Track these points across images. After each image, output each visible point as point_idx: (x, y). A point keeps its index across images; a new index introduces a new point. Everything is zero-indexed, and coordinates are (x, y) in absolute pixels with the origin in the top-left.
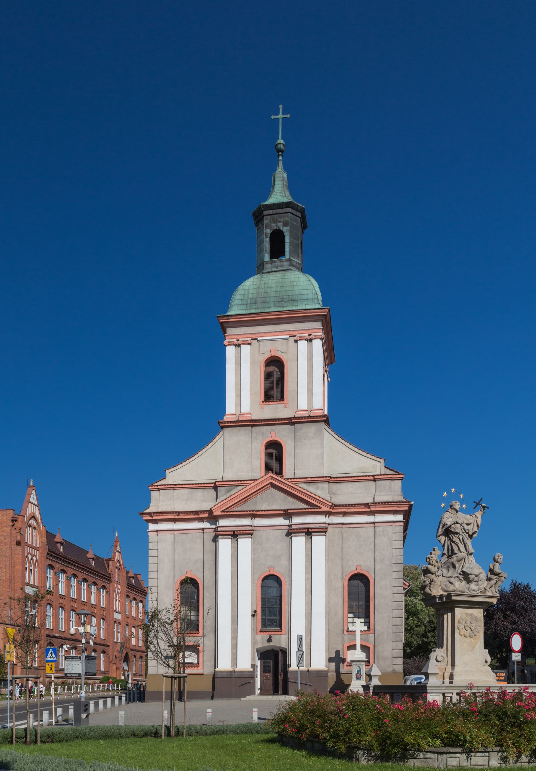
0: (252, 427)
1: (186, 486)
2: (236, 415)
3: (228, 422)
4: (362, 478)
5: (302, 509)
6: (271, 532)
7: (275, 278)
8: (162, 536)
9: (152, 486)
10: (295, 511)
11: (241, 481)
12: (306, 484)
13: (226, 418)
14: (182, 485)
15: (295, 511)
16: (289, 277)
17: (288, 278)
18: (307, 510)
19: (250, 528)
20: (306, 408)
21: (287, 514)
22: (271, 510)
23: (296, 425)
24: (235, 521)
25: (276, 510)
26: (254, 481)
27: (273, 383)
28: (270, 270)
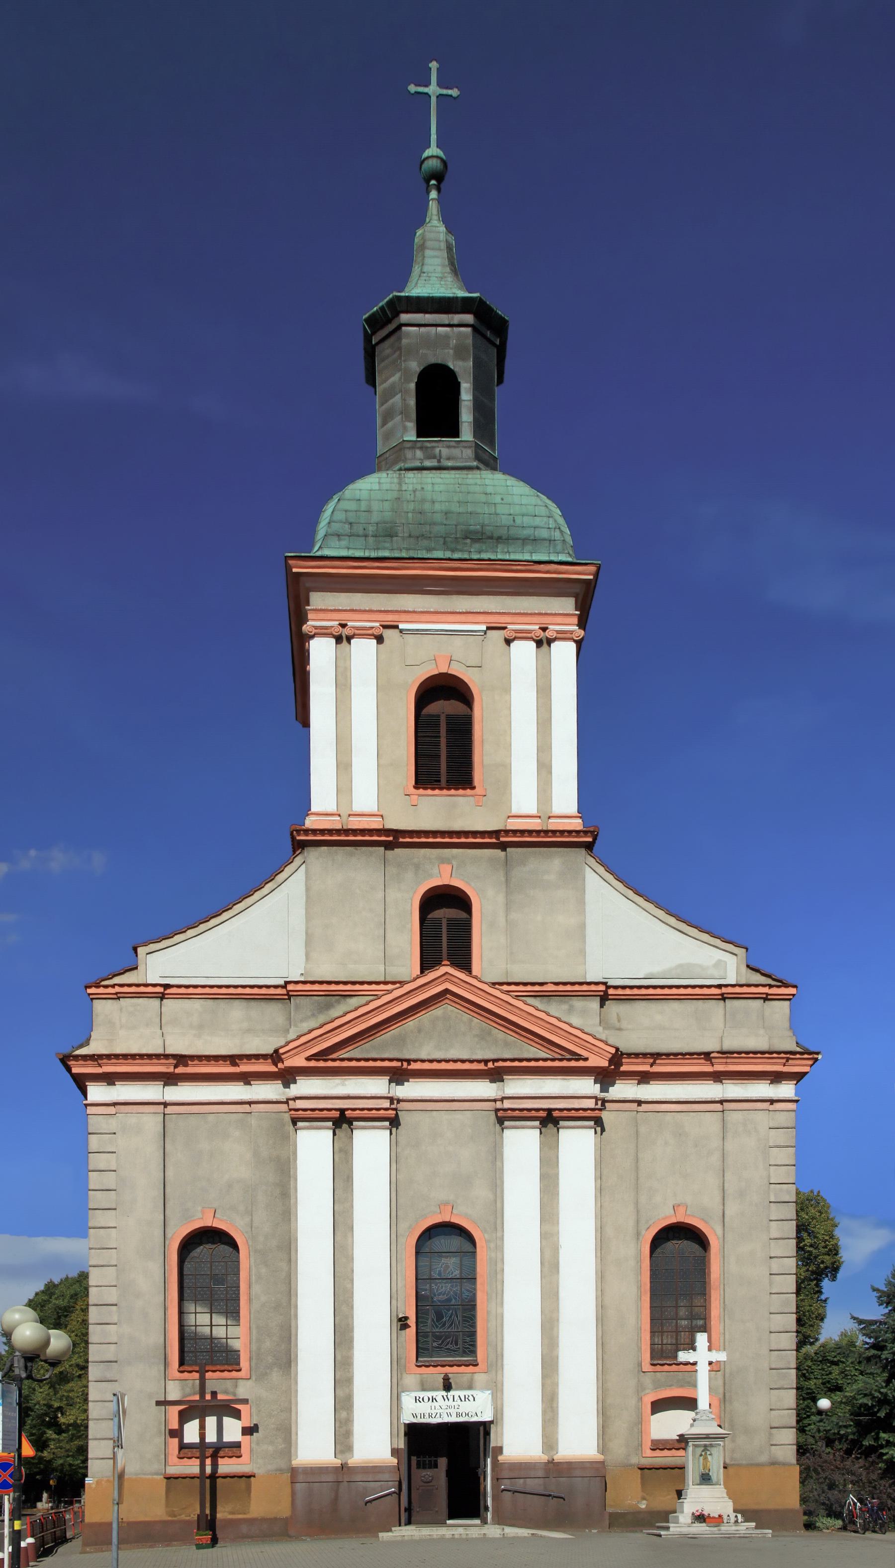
0: (386, 849)
1: (199, 990)
2: (339, 815)
3: (315, 832)
7: (439, 480)
8: (131, 1118)
9: (98, 987)
12: (538, 998)
13: (310, 822)
14: (187, 987)
16: (479, 481)
17: (476, 484)
18: (549, 1064)
19: (386, 1104)
20: (534, 812)
23: (508, 849)
24: (343, 1085)
27: (438, 744)
28: (418, 464)
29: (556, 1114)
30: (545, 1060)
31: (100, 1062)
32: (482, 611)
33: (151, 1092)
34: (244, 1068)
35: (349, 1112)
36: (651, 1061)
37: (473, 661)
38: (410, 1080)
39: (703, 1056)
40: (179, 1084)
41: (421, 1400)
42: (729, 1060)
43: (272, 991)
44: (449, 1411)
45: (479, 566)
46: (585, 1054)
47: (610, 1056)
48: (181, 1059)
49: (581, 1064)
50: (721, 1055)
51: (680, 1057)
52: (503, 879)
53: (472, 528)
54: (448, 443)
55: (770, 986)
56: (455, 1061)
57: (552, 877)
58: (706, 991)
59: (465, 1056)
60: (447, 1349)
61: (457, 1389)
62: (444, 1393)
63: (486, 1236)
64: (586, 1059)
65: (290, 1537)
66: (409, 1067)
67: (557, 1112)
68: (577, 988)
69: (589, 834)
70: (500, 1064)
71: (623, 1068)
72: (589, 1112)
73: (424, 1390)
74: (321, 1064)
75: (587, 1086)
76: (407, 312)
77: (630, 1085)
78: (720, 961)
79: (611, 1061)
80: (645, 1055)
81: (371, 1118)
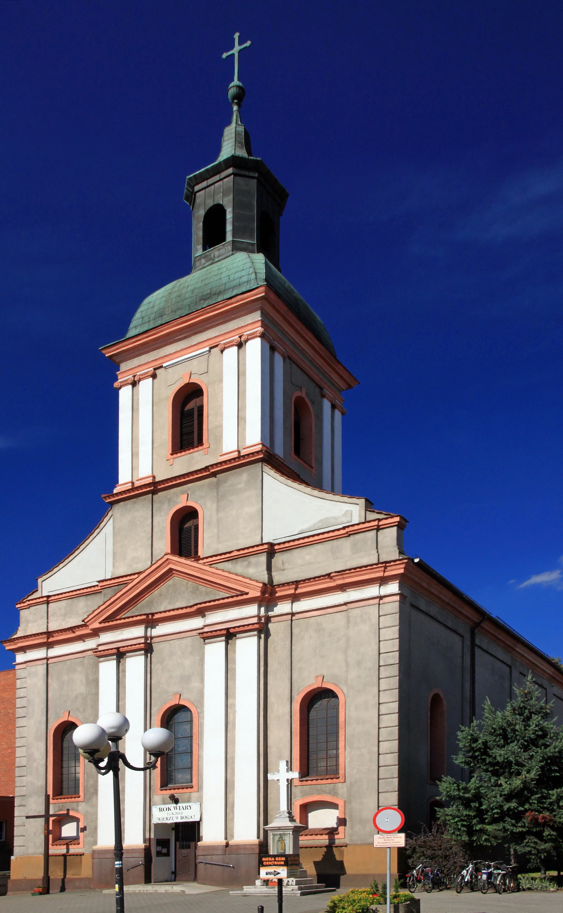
5: (219, 600)
10: (208, 604)
15: (208, 604)
22: (173, 610)
23: (217, 476)
25: (182, 608)
29: (232, 631)
30: (228, 598)
31: (15, 642)
32: (206, 339)
33: (40, 653)
34: (78, 633)
36: (294, 586)
38: (159, 624)
39: (327, 577)
40: (54, 647)
41: (162, 810)
42: (344, 576)
44: (177, 815)
45: (198, 314)
47: (260, 589)
48: (49, 634)
49: (245, 597)
50: (337, 574)
51: (312, 580)
53: (205, 293)
54: (218, 248)
55: (379, 520)
56: (178, 609)
57: (242, 485)
59: (185, 605)
60: (185, 779)
61: (182, 803)
62: (175, 805)
63: (198, 710)
64: (247, 594)
65: (90, 889)
66: (154, 618)
67: (232, 629)
68: (251, 550)
69: (260, 453)
70: (199, 606)
71: (277, 595)
72: (251, 626)
73: (164, 804)
74: (107, 624)
75: (252, 610)
76: (197, 184)
77: (287, 604)
78: (347, 511)
79: (263, 592)
80: (288, 584)
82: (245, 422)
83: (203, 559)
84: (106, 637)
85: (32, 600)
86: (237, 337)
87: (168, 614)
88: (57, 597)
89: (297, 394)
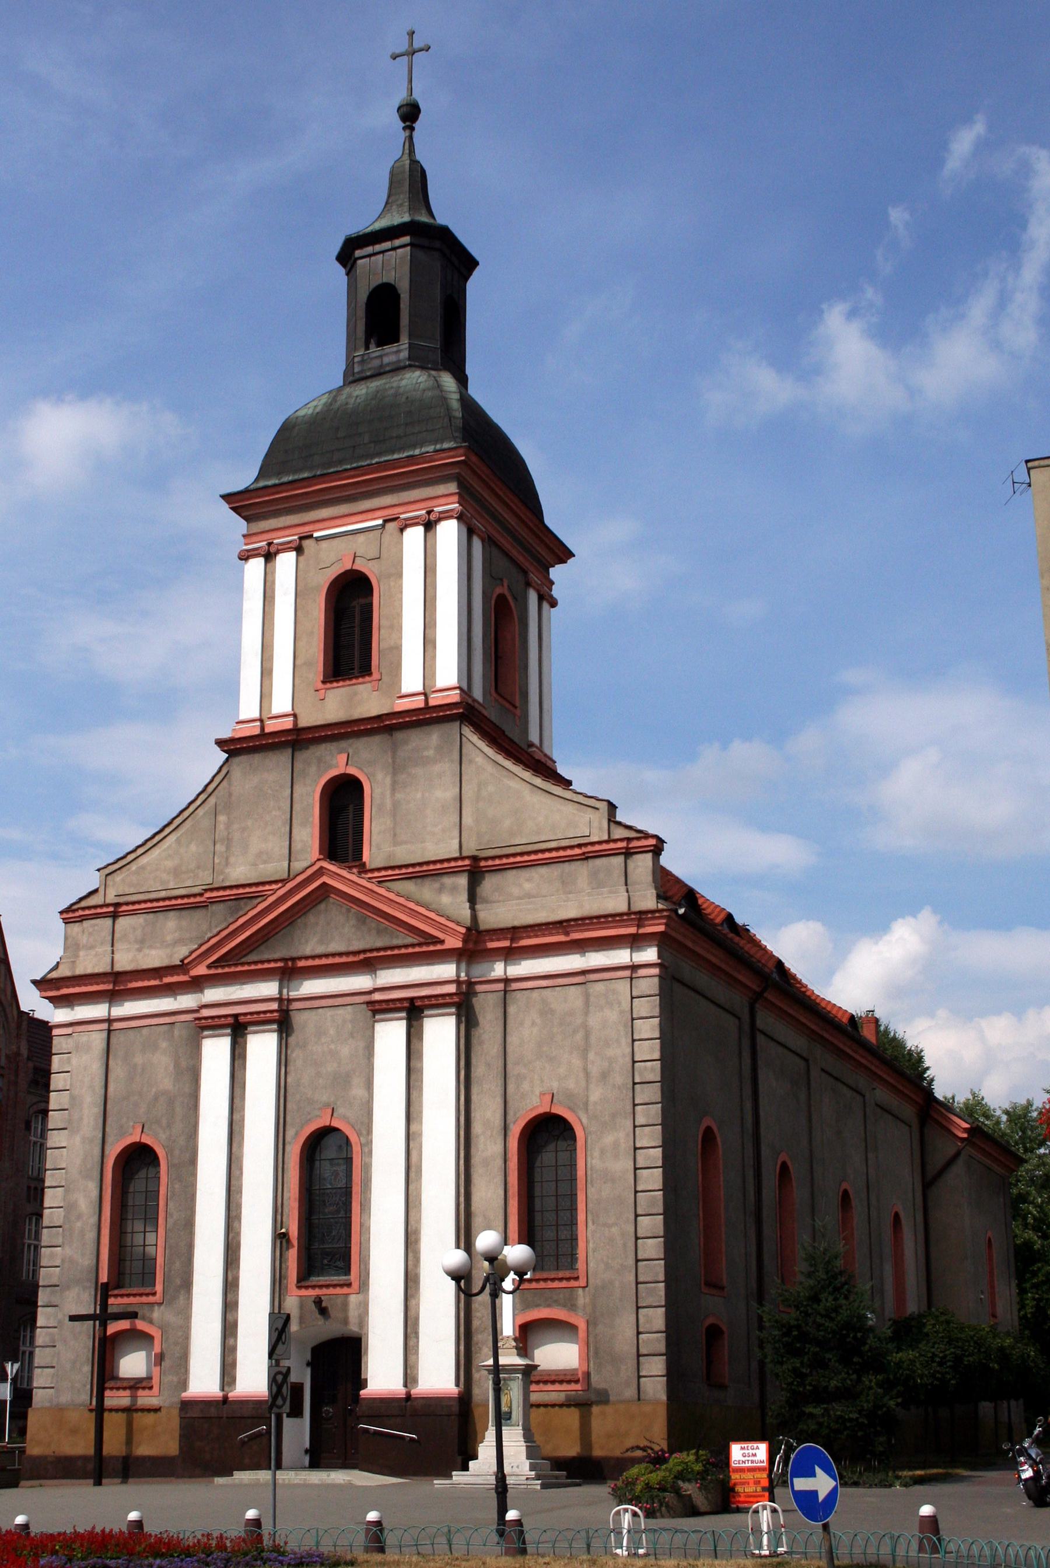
4: (554, 854)
6: (329, 1013)
11: (263, 884)
12: (414, 880)
21: (367, 963)
22: (327, 956)
25: (340, 954)
26: (280, 885)
35: (242, 1017)
37: (373, 553)
43: (198, 899)
46: (441, 936)
48: (116, 976)
52: (390, 760)
57: (431, 753)
58: (569, 852)
70: (369, 955)
81: (261, 1021)
82: (435, 647)
83: (372, 871)
84: (213, 994)
85: (89, 908)
86: (424, 512)
87: (317, 962)
88: (131, 907)
89: (498, 590)
